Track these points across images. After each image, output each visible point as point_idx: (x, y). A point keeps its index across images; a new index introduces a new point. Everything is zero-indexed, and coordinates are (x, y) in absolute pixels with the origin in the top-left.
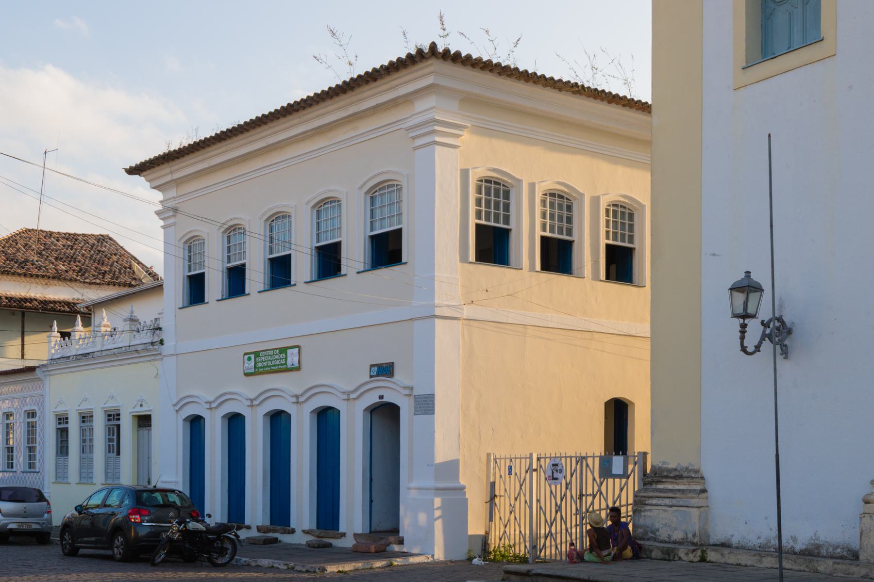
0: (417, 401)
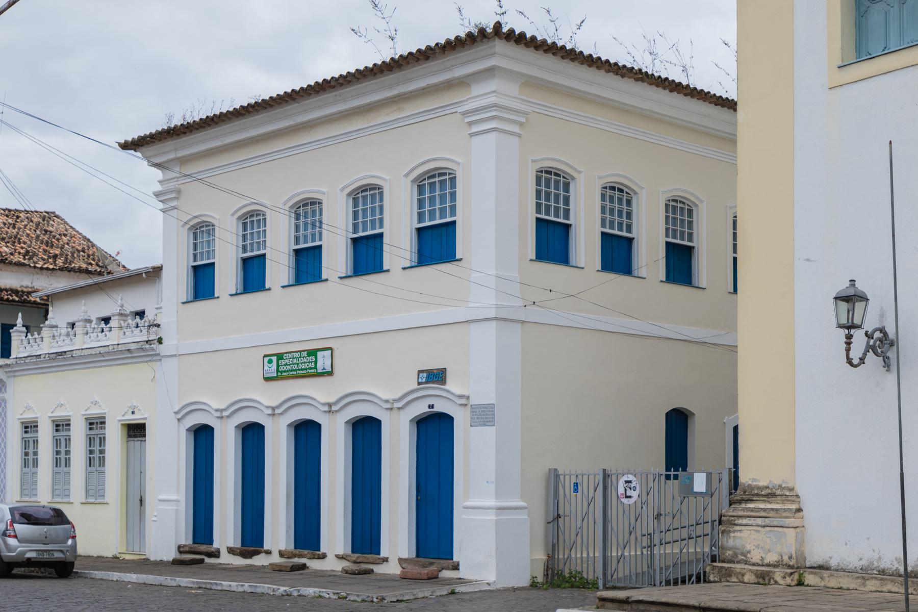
0: (474, 412)
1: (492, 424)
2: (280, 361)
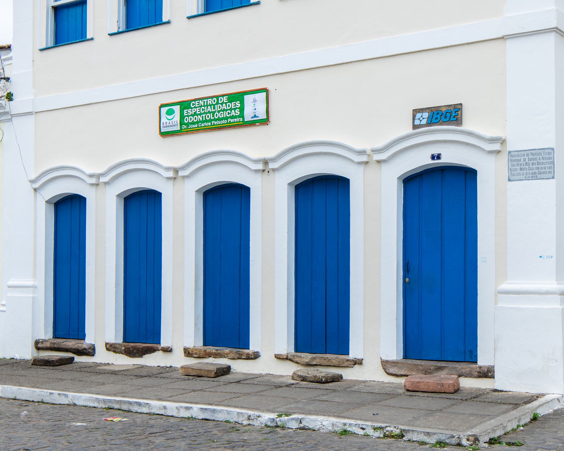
0: (515, 160)
1: (551, 175)
2: (185, 110)
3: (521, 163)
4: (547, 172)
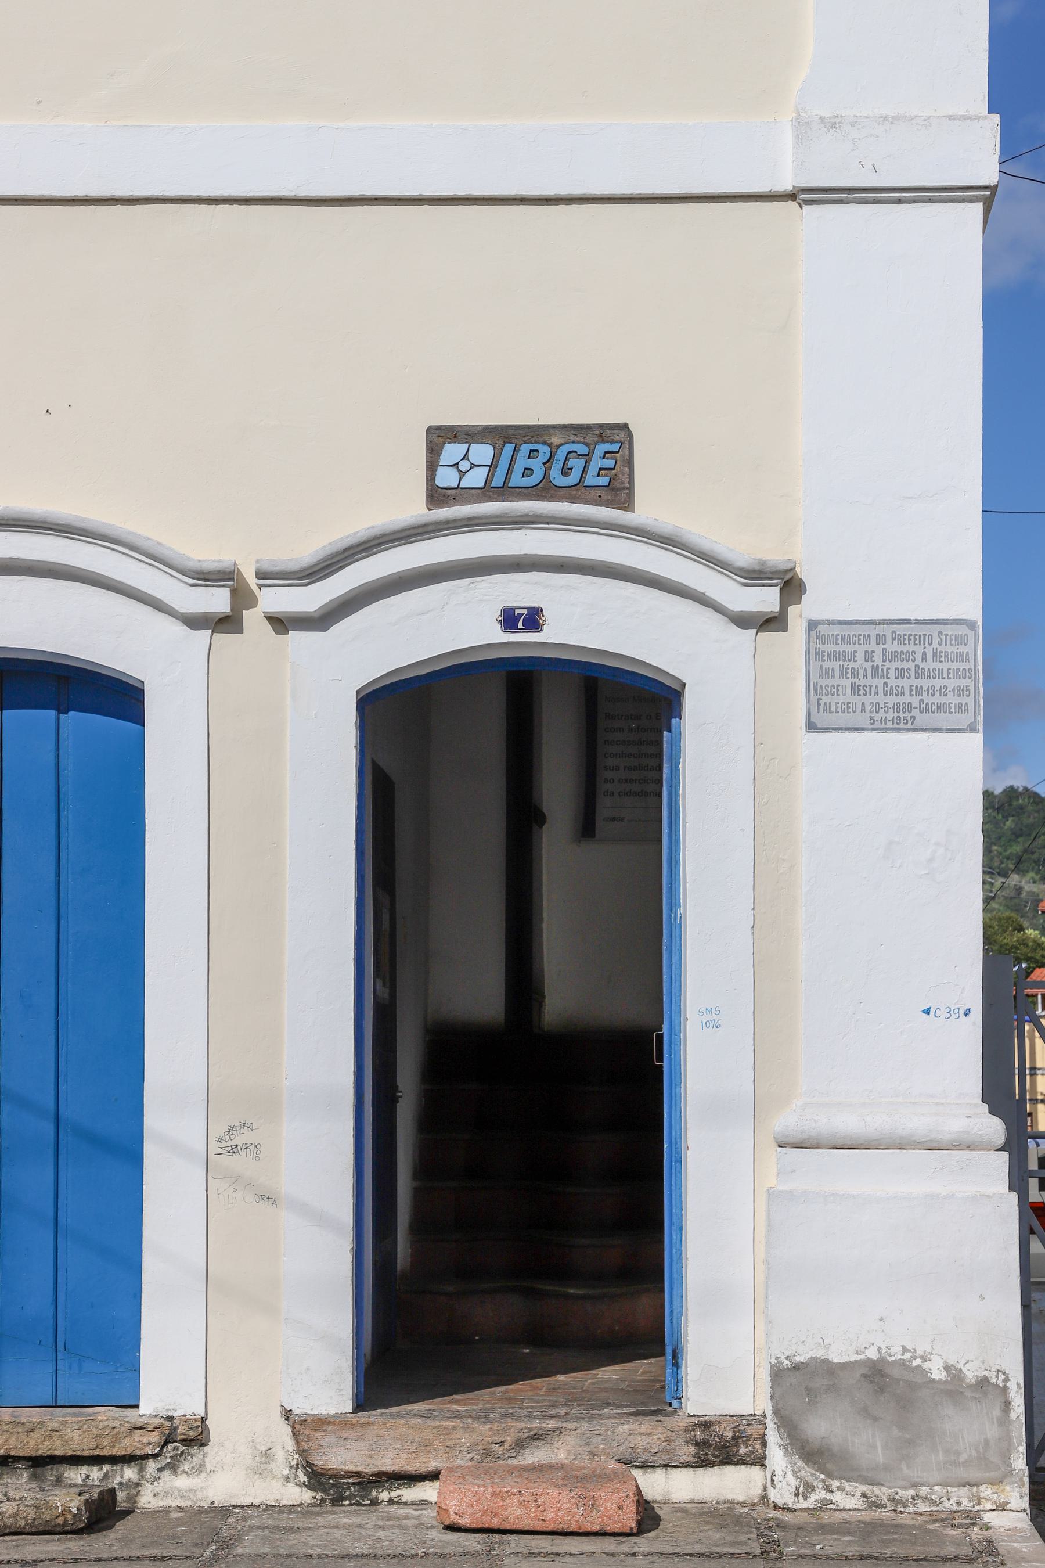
0: (833, 656)
3: (856, 665)
4: (950, 708)
